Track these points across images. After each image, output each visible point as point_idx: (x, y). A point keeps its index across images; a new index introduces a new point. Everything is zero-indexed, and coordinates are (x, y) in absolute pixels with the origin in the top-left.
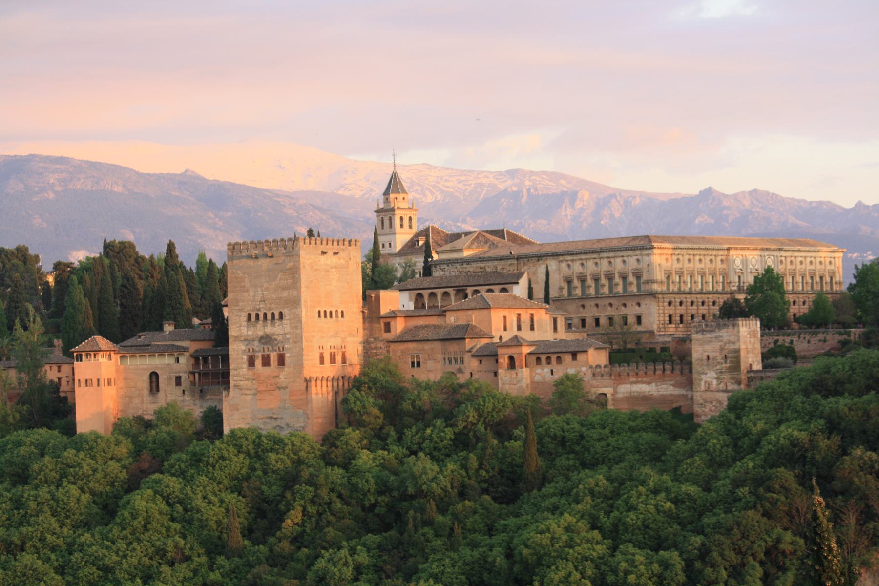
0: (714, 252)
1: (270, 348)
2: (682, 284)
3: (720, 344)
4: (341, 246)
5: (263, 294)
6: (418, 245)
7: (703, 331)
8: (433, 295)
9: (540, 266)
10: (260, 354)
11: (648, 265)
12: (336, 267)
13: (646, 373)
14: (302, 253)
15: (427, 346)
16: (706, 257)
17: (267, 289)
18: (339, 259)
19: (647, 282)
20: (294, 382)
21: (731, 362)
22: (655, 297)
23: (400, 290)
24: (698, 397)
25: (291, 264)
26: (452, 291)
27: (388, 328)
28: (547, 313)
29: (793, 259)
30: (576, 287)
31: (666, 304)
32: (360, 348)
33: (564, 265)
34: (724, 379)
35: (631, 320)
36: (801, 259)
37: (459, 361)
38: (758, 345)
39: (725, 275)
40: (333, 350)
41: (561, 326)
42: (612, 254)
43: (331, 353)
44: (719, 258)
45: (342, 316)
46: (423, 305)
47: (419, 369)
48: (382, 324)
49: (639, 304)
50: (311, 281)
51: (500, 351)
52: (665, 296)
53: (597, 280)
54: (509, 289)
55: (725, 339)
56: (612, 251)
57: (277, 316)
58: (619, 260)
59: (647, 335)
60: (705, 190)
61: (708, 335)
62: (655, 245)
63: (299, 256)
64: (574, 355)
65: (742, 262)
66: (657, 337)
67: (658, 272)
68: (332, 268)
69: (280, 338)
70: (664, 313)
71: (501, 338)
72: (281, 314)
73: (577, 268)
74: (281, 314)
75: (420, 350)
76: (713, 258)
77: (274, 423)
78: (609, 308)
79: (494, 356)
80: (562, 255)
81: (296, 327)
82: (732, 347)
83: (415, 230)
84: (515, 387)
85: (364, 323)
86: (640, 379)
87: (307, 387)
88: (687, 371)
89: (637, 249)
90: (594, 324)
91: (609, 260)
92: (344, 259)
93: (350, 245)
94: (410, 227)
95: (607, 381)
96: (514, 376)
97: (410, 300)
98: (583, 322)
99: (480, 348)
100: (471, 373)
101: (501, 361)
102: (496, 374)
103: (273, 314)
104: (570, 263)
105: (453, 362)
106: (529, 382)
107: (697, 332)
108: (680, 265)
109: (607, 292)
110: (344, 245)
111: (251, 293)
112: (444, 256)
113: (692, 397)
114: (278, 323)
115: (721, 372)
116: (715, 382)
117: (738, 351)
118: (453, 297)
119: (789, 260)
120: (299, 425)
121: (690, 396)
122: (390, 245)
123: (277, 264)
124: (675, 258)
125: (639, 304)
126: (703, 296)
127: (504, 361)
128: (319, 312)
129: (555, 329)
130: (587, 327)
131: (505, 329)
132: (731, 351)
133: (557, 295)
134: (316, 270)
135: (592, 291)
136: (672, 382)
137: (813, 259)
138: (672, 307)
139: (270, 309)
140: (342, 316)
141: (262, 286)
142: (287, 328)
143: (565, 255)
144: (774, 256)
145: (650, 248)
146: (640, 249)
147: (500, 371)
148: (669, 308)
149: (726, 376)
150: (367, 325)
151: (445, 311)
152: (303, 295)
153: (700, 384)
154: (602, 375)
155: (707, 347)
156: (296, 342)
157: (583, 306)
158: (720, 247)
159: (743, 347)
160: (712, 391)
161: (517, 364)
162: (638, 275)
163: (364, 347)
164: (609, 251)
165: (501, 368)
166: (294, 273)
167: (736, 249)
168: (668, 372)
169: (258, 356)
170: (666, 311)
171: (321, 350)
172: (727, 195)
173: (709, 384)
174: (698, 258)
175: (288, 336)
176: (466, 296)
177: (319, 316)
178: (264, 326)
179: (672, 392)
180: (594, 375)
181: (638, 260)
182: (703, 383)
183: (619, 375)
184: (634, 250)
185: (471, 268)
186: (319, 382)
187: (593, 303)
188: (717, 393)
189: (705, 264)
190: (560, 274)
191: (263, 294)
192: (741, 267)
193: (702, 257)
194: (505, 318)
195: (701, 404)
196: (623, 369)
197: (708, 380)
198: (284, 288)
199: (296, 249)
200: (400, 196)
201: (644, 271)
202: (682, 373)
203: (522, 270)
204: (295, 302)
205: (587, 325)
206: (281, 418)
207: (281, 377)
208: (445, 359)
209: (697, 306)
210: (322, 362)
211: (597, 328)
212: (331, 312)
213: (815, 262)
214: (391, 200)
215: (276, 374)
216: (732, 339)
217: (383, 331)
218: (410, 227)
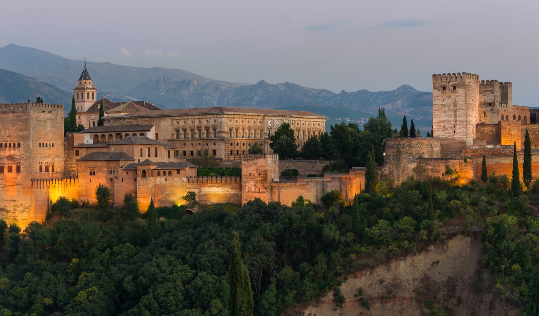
0: (256, 117)
1: (12, 162)
2: (238, 134)
3: (257, 167)
4: (53, 108)
5: (9, 133)
6: (97, 108)
7: (248, 160)
8: (103, 136)
9: (162, 122)
10: (6, 166)
11: (220, 123)
12: (50, 119)
13: (216, 182)
14: (32, 111)
15: (99, 164)
16: (252, 120)
17: (11, 130)
18: (52, 115)
19: (220, 132)
20: (25, 181)
21: (262, 177)
22: (224, 141)
23: (85, 133)
24: (244, 195)
25: (25, 117)
26: (114, 134)
27: (77, 154)
28: (164, 148)
29: (299, 122)
30: (181, 134)
31: (229, 144)
32: (63, 164)
33: (175, 122)
34: (258, 186)
35: (210, 152)
36: (303, 122)
37: (116, 172)
38: (277, 168)
39: (262, 130)
40: (47, 165)
41: (172, 155)
42: (201, 117)
43: (46, 166)
44: (259, 120)
45: (53, 146)
46: (98, 141)
47: (94, 176)
48: (75, 151)
49: (215, 144)
50: (36, 127)
51: (138, 167)
52: (229, 140)
53: (192, 130)
54: (145, 134)
55: (260, 164)
56: (201, 115)
57: (16, 145)
58: (204, 120)
59: (218, 161)
60: (260, 82)
61: (251, 162)
62: (225, 112)
63: (29, 113)
64: (178, 171)
65: (271, 123)
66: (224, 162)
67: (226, 127)
68: (47, 120)
69: (18, 157)
70: (228, 149)
71: (139, 160)
72: (19, 144)
73: (182, 123)
74: (19, 144)
75: (95, 166)
76: (255, 120)
77: (13, 204)
78: (199, 146)
79: (135, 171)
80: (174, 116)
81: (27, 152)
82: (263, 169)
83: (95, 100)
84: (146, 187)
85: (65, 150)
86: (213, 185)
87: (32, 184)
88: (239, 181)
89: (215, 114)
90: (190, 154)
91: (200, 120)
92: (54, 115)
93: (58, 108)
94: (93, 98)
95: (195, 185)
96: (146, 181)
97: (91, 138)
98: (185, 152)
99: (128, 165)
100: (122, 179)
101: (139, 173)
102: (136, 180)
103: (14, 144)
104: (178, 121)
105: (113, 172)
106: (153, 184)
107: (244, 161)
108: (238, 124)
109: (198, 137)
110: (54, 107)
111: (3, 132)
112: (110, 115)
113: (241, 195)
114: (17, 149)
115: (257, 182)
116: (253, 187)
117: (266, 171)
118: (114, 138)
119: (297, 122)
120: (27, 205)
121: (240, 194)
122: (82, 107)
123: (17, 117)
124: (235, 120)
125: (215, 144)
126: (250, 141)
127: (140, 173)
128: (40, 143)
129: (169, 156)
130: (186, 156)
131: (141, 156)
132: (262, 171)
133: (171, 138)
134: (39, 121)
135: (190, 136)
136: (231, 187)
137: (310, 122)
138: (233, 146)
139: (13, 141)
140: (53, 146)
141: (9, 128)
142: (22, 152)
143: (176, 116)
144: (288, 120)
145: (221, 114)
146: (216, 114)
147: (138, 178)
148: (231, 147)
149: (260, 184)
150: (66, 151)
151: (109, 145)
152: (31, 134)
153: (246, 188)
154: (193, 183)
155: (250, 168)
156: (26, 160)
157: (185, 144)
158: (260, 114)
159: (269, 169)
160: (252, 192)
161: (147, 175)
162: (215, 128)
163: (64, 163)
164: (200, 115)
165: (138, 177)
166: (26, 122)
167: (268, 116)
168: (228, 181)
169: (5, 167)
170: (229, 148)
171: (41, 165)
172: (272, 85)
173: (250, 189)
174: (247, 120)
175: (22, 156)
176: (121, 137)
177: (40, 146)
178: (9, 150)
179: (231, 192)
180: (189, 181)
181: (215, 120)
182: (247, 188)
183: (202, 182)
184: (213, 115)
185: (125, 123)
186: (39, 182)
187: (190, 143)
188: (254, 193)
189: (251, 123)
190: (172, 127)
191: (9, 133)
192: (270, 125)
193: (249, 120)
194: (141, 149)
195: (246, 199)
196: (205, 179)
197: (249, 186)
198: (21, 130)
199: (28, 109)
200: (88, 82)
201: (218, 126)
202: (236, 182)
203: (152, 124)
204: (26, 138)
205: (186, 154)
206: (18, 201)
207: (18, 178)
208: (108, 171)
209: (246, 146)
210: (41, 171)
211: (192, 156)
212: (46, 144)
213: (311, 124)
214: (83, 83)
215: (15, 177)
216: (264, 165)
217: (75, 155)
218: (93, 98)
